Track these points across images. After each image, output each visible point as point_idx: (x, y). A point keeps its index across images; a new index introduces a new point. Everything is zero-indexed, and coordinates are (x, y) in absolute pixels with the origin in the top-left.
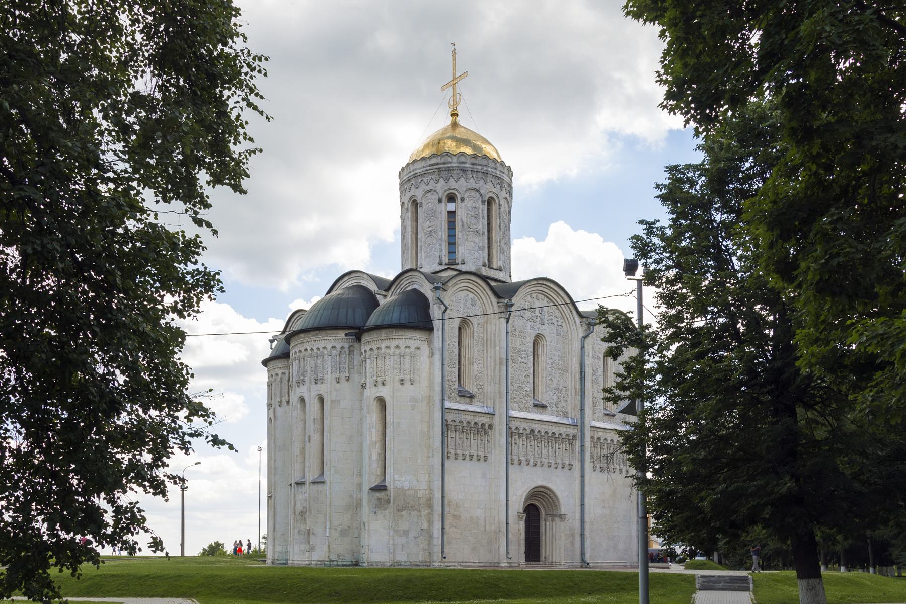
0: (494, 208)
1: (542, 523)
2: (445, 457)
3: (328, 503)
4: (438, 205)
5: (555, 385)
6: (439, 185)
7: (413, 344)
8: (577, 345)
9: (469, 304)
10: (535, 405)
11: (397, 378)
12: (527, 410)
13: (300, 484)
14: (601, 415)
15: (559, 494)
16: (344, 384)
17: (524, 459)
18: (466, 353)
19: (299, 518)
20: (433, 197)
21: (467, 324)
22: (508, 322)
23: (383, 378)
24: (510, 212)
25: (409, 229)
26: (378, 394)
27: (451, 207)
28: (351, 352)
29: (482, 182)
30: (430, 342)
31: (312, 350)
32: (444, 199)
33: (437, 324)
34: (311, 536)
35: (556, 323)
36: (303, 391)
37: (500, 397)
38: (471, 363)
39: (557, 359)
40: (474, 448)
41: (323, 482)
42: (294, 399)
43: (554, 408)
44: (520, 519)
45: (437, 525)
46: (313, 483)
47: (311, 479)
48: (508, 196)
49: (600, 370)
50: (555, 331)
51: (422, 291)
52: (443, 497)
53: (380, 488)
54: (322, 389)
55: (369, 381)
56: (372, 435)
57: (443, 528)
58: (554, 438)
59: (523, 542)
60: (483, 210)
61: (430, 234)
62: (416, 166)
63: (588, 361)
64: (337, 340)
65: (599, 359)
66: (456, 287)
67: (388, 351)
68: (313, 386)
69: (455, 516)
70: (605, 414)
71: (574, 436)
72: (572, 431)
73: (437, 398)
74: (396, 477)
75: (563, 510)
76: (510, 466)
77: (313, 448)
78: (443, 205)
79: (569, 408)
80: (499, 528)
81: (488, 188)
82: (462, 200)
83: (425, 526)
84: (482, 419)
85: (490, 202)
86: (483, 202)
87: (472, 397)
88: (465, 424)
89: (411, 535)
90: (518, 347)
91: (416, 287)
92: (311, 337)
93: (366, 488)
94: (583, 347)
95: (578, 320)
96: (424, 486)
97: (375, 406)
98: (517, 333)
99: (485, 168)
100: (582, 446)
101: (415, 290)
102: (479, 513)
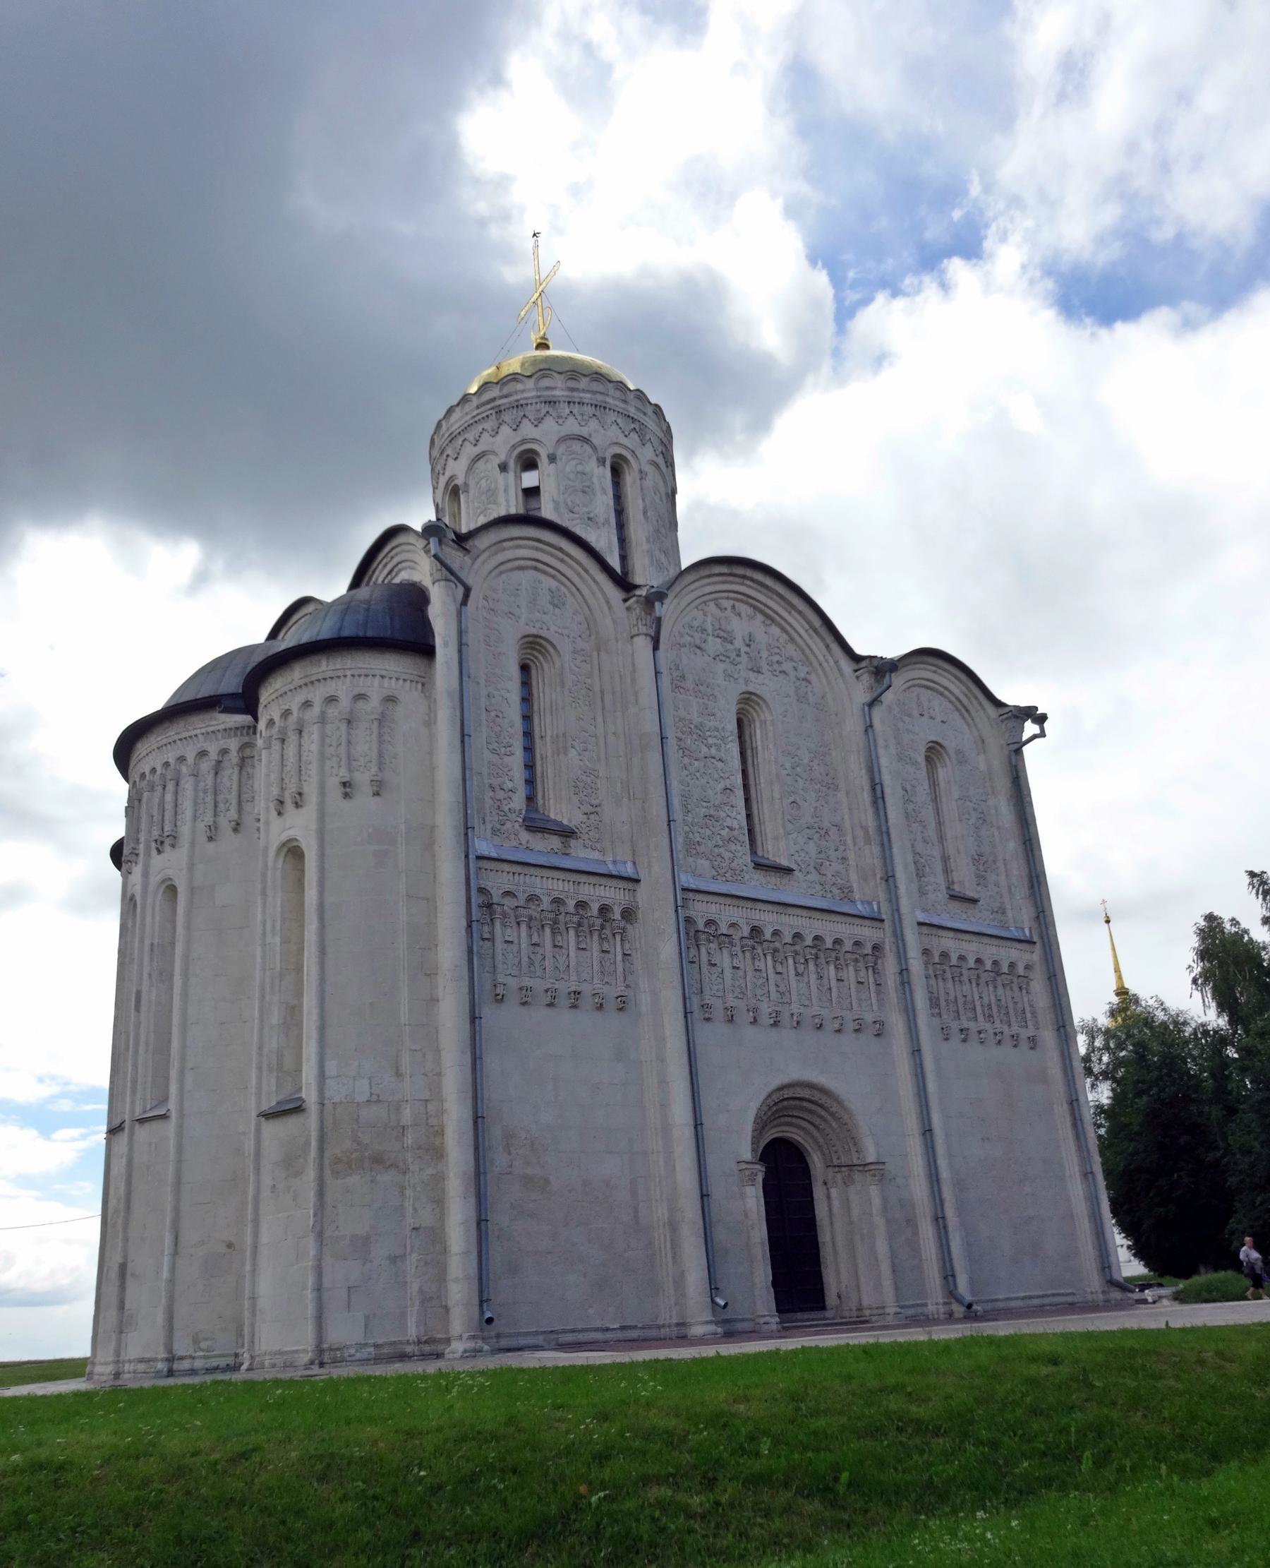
0: (630, 479)
4: (500, 477)
6: (499, 438)
8: (853, 725)
10: (758, 866)
14: (942, 895)
18: (545, 727)
21: (544, 652)
27: (530, 479)
29: (593, 424)
30: (425, 683)
31: (153, 770)
32: (512, 464)
35: (792, 673)
43: (814, 876)
49: (923, 790)
63: (886, 761)
65: (915, 763)
66: (502, 557)
68: (157, 861)
71: (876, 947)
78: (511, 475)
79: (854, 877)
81: (609, 436)
84: (600, 891)
86: (602, 461)
87: (567, 834)
90: (696, 719)
94: (869, 727)
99: (599, 397)
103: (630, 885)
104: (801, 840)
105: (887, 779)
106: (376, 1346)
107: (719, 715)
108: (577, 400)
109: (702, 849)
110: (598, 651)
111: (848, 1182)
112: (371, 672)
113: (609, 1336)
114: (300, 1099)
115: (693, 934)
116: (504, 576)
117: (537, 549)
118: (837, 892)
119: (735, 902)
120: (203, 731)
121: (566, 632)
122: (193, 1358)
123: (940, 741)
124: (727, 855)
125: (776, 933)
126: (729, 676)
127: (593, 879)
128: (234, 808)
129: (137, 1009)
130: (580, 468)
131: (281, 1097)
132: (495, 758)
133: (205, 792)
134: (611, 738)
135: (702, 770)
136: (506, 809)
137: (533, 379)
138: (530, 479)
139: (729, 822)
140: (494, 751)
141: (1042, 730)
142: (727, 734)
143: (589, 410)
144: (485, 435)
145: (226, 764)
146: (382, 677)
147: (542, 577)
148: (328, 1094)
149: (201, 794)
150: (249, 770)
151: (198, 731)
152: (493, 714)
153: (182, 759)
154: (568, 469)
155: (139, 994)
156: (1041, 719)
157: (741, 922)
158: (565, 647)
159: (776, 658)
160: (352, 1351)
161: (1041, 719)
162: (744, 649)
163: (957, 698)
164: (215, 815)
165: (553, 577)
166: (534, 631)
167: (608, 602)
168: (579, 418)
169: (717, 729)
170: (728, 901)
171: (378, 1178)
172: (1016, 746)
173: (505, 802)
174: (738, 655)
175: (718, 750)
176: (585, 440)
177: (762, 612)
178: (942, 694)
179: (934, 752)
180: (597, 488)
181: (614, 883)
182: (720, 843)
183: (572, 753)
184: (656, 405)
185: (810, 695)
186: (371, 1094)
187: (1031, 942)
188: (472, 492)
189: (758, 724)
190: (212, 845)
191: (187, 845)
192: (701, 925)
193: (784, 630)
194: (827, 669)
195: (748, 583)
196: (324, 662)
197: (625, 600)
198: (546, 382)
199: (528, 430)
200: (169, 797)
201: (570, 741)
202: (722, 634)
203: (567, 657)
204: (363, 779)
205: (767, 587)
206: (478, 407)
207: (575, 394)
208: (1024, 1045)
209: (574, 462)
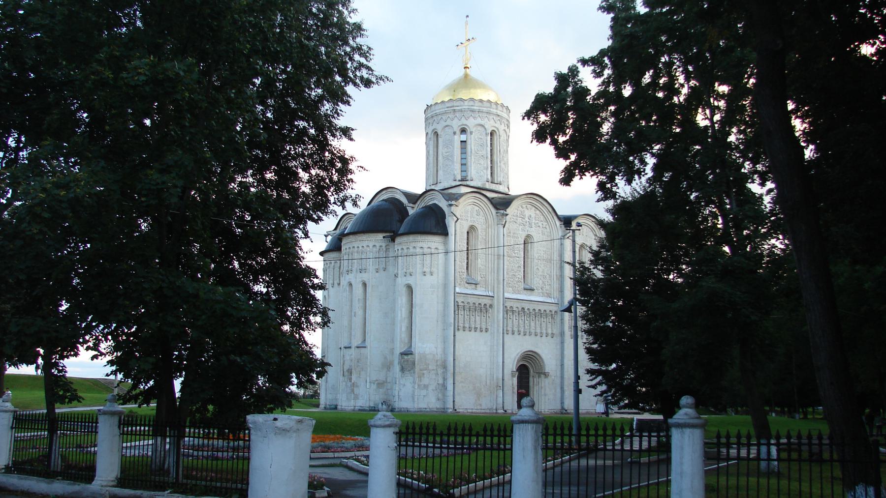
1: (531, 379)
2: (456, 329)
5: (540, 273)
7: (433, 245)
17: (516, 329)
19: (346, 374)
23: (411, 270)
24: (508, 140)
25: (431, 152)
28: (387, 250)
29: (486, 119)
30: (445, 244)
32: (458, 132)
33: (451, 230)
36: (351, 277)
37: (498, 283)
40: (478, 322)
42: (344, 282)
44: (513, 376)
54: (365, 276)
56: (402, 313)
58: (540, 314)
61: (446, 158)
62: (437, 107)
64: (374, 242)
75: (547, 369)
77: (358, 321)
78: (456, 137)
81: (490, 125)
82: (471, 133)
83: (441, 381)
86: (487, 134)
89: (431, 388)
93: (398, 352)
96: (440, 351)
97: (404, 290)
111: (539, 377)
115: (506, 311)
126: (523, 230)
198: (471, 103)
199: (464, 121)
204: (427, 270)
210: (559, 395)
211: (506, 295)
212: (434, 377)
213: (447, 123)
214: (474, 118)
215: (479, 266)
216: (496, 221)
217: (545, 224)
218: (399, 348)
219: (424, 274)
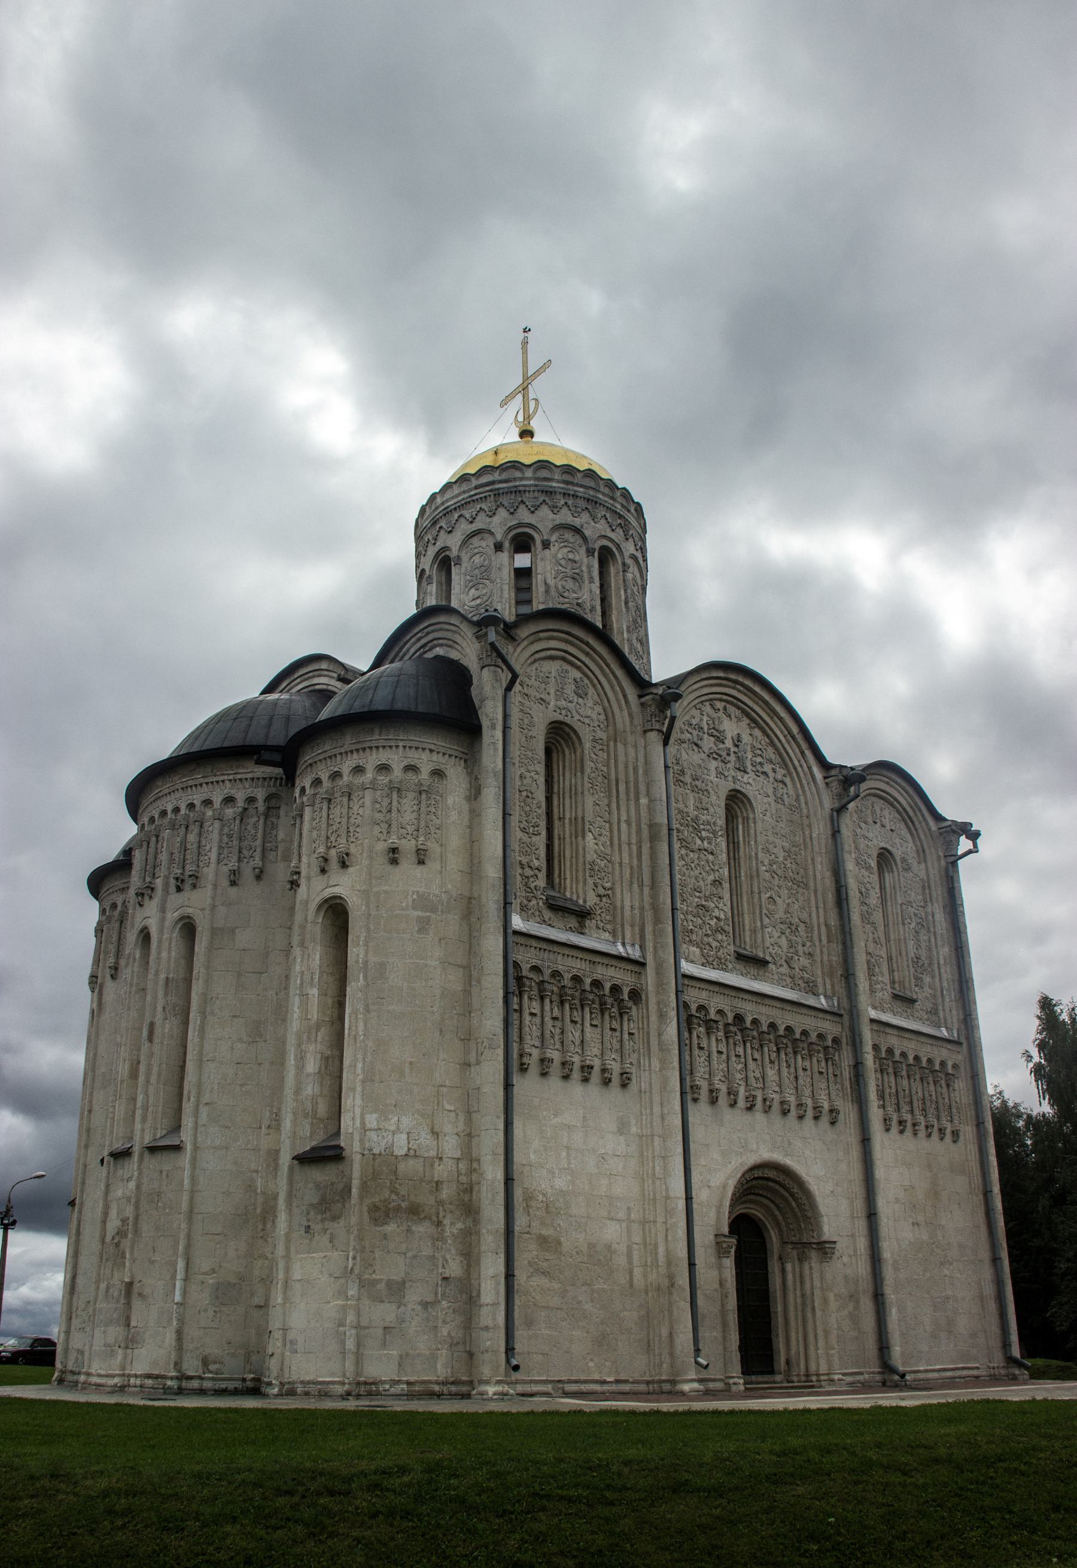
1: (774, 1267)
2: (513, 1067)
3: (185, 1206)
5: (780, 914)
6: (496, 520)
7: (426, 762)
8: (820, 830)
9: (570, 689)
10: (740, 957)
11: (381, 846)
12: (722, 966)
13: (121, 1155)
14: (887, 996)
15: (813, 1186)
16: (250, 888)
18: (565, 808)
20: (484, 544)
21: (567, 738)
22: (666, 743)
24: (644, 589)
26: (328, 893)
27: (523, 560)
29: (585, 516)
30: (471, 759)
31: (177, 810)
32: (507, 544)
33: (490, 712)
34: (137, 1304)
35: (771, 774)
37: (657, 920)
38: (580, 828)
39: (781, 856)
41: (177, 1148)
43: (784, 969)
44: (720, 1251)
45: (492, 1267)
46: (153, 1150)
47: (147, 1140)
48: (639, 555)
50: (770, 791)
51: (454, 655)
52: (509, 1180)
53: (325, 1155)
55: (308, 864)
57: (509, 1276)
58: (791, 1042)
59: (733, 1319)
60: (589, 567)
63: (850, 866)
65: (868, 868)
67: (359, 780)
68: (175, 899)
69: (543, 1241)
70: (896, 997)
71: (836, 1040)
72: (830, 1028)
73: (491, 900)
74: (372, 1121)
75: (829, 1230)
76: (690, 1105)
78: (504, 556)
80: (671, 1277)
81: (596, 528)
82: (546, 545)
83: (455, 1268)
84: (611, 972)
85: (605, 556)
86: (590, 552)
87: (582, 915)
88: (567, 981)
89: (414, 1296)
91: (439, 651)
92: (178, 780)
95: (818, 774)
96: (451, 1146)
98: (688, 779)
99: (591, 493)
100: (858, 1066)
101: (437, 658)
102: (612, 1232)
103: (637, 969)
104: (776, 934)
105: (852, 884)
106: (408, 1383)
107: (711, 810)
108: (572, 493)
109: (694, 937)
110: (615, 741)
112: (421, 745)
113: (606, 1388)
114: (339, 1147)
116: (536, 664)
117: (566, 641)
118: (803, 985)
119: (722, 990)
120: (231, 777)
121: (587, 721)
122: (201, 1378)
123: (890, 848)
124: (714, 944)
125: (755, 1022)
127: (605, 960)
128: (258, 855)
129: (150, 1039)
130: (571, 556)
131: (314, 1143)
132: (525, 838)
133: (230, 836)
134: (624, 826)
135: (696, 862)
136: (532, 886)
137: (532, 469)
138: (523, 560)
139: (716, 913)
140: (523, 830)
141: (975, 845)
142: (718, 828)
143: (582, 504)
144: (482, 514)
145: (251, 811)
146: (431, 751)
147: (569, 668)
148: (367, 1145)
149: (225, 839)
150: (274, 820)
151: (226, 777)
152: (524, 794)
153: (208, 803)
154: (560, 556)
155: (152, 1025)
156: (974, 836)
157: (727, 1009)
158: (586, 735)
159: (759, 759)
160: (387, 1387)
161: (974, 836)
162: (733, 749)
163: (904, 809)
164: (240, 860)
165: (578, 668)
166: (561, 718)
167: (625, 696)
168: (573, 509)
169: (709, 823)
170: (716, 989)
171: (413, 1228)
172: (953, 859)
173: (532, 879)
174: (728, 755)
175: (709, 843)
176: (577, 531)
177: (748, 716)
178: (891, 804)
179: (885, 858)
180: (586, 575)
181: (623, 965)
182: (709, 932)
183: (589, 837)
184: (638, 504)
185: (785, 796)
186: (409, 1149)
187: (958, 1043)
188: (464, 565)
189: (740, 820)
190: (235, 889)
191: (210, 887)
192: (694, 1007)
193: (764, 732)
194: (802, 774)
195: (739, 687)
196: (372, 731)
197: (640, 697)
198: (544, 473)
199: (524, 515)
200: (192, 837)
201: (587, 826)
202: (715, 733)
203: (587, 745)
204: (408, 846)
205: (754, 693)
206: (476, 488)
207: (571, 487)
208: (948, 1137)
209: (565, 550)
210: (869, 1323)
211: (686, 967)
212: (427, 1251)
213: (478, 525)
214: (554, 509)
215: (589, 858)
216: (638, 720)
217: (781, 772)
218: (295, 1134)
219: (394, 855)
